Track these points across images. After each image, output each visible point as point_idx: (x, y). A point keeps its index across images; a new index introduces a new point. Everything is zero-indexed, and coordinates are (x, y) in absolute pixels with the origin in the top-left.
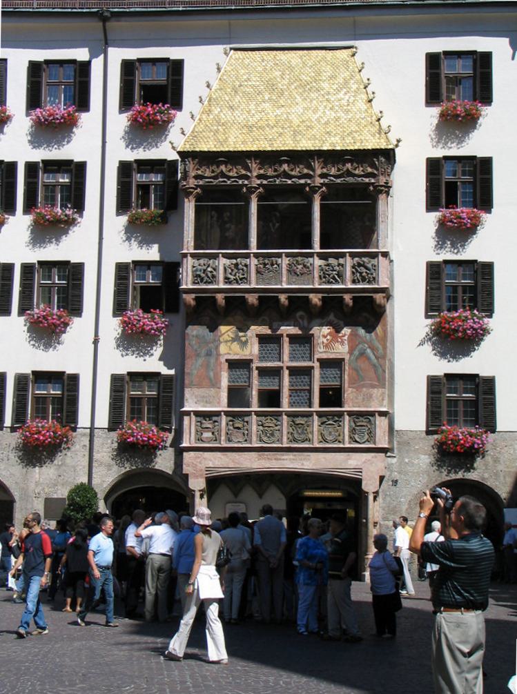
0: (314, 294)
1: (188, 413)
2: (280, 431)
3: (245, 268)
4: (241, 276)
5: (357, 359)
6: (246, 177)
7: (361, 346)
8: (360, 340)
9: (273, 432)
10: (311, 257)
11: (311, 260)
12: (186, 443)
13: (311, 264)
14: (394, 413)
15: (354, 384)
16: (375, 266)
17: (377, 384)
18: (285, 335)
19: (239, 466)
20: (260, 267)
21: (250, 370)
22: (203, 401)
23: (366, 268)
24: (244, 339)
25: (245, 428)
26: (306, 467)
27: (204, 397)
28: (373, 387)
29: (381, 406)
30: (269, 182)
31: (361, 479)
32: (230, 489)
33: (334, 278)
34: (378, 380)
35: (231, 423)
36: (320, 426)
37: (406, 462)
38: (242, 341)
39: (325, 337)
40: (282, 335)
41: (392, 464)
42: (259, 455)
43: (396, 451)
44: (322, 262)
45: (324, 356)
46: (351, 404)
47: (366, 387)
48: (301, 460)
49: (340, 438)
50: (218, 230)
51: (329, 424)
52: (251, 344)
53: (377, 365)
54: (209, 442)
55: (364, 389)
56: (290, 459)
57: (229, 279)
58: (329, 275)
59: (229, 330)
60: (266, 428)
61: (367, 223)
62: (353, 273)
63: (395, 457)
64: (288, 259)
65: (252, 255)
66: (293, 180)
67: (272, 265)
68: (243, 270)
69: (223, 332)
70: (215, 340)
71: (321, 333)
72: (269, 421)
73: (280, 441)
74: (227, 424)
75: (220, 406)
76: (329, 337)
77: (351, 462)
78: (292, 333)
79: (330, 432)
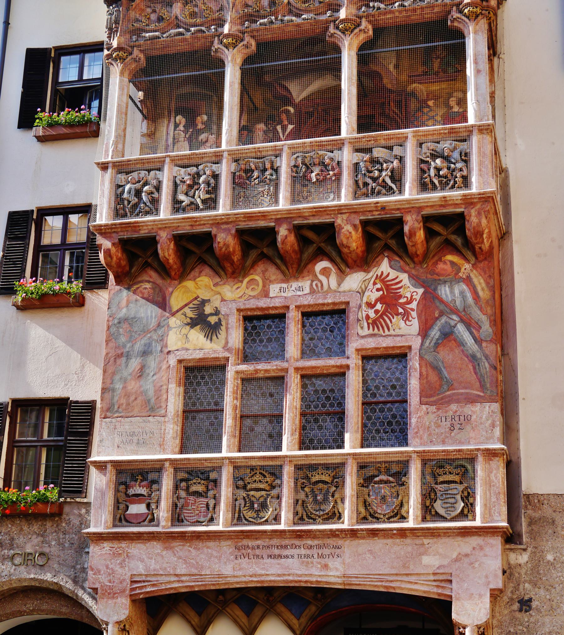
0: (345, 216)
1: (101, 466)
2: (279, 497)
3: (212, 181)
4: (204, 196)
5: (437, 345)
6: (220, 23)
7: (444, 319)
8: (442, 307)
9: (266, 499)
10: (340, 149)
11: (336, 154)
12: (95, 526)
13: (338, 162)
14: (519, 458)
15: (431, 396)
16: (466, 154)
17: (482, 394)
18: (292, 307)
19: (194, 571)
20: (240, 177)
21: (223, 383)
22: (131, 442)
23: (446, 159)
24: (213, 320)
25: (211, 493)
26: (331, 574)
27: (133, 434)
28: (472, 400)
29: (488, 439)
30: (260, 24)
31: (451, 597)
32: (189, 622)
33: (384, 185)
34: (482, 387)
35: (183, 484)
36: (363, 486)
37: (549, 562)
38: (209, 324)
39: (370, 305)
40: (288, 307)
41: (520, 565)
42: (238, 548)
43: (524, 540)
44: (357, 157)
45: (371, 343)
46: (425, 437)
47: (458, 401)
48: (321, 556)
49: (403, 512)
50: (186, 144)
51: (381, 482)
52: (227, 329)
53: (479, 355)
54: (139, 524)
55: (454, 407)
56: (300, 556)
57: (183, 202)
58: (374, 179)
59: (186, 305)
60: (252, 493)
61: (456, 109)
62: (423, 171)
63: (525, 550)
64: (295, 156)
65: (225, 154)
66: (303, 16)
67: (265, 170)
68: (208, 184)
69: (175, 309)
70: (159, 325)
71: (365, 300)
72: (258, 477)
73: (277, 519)
74: (176, 487)
75: (164, 451)
76: (379, 306)
77: (426, 560)
78: (306, 303)
79: (384, 498)
